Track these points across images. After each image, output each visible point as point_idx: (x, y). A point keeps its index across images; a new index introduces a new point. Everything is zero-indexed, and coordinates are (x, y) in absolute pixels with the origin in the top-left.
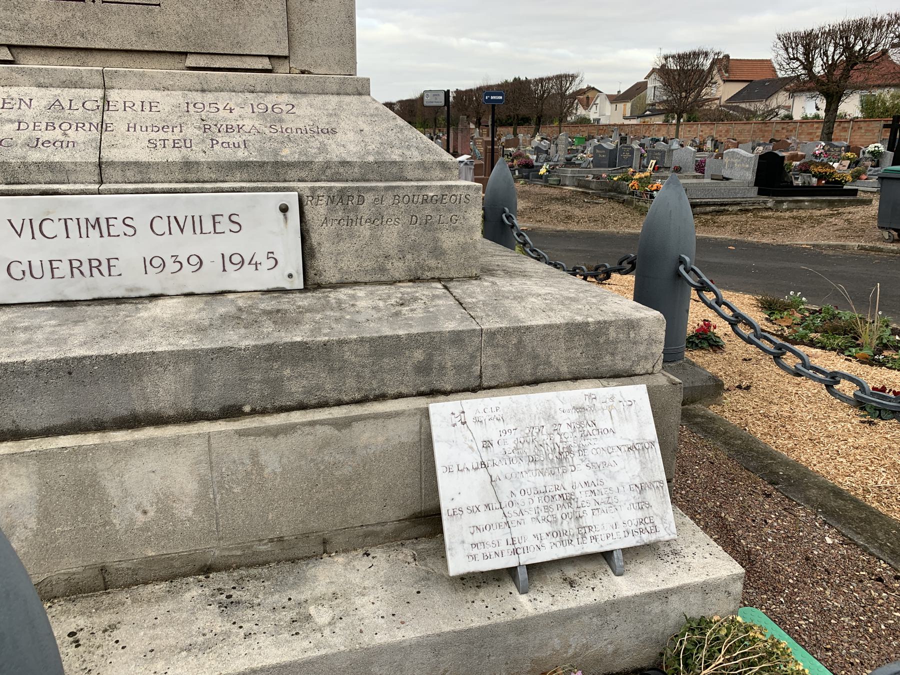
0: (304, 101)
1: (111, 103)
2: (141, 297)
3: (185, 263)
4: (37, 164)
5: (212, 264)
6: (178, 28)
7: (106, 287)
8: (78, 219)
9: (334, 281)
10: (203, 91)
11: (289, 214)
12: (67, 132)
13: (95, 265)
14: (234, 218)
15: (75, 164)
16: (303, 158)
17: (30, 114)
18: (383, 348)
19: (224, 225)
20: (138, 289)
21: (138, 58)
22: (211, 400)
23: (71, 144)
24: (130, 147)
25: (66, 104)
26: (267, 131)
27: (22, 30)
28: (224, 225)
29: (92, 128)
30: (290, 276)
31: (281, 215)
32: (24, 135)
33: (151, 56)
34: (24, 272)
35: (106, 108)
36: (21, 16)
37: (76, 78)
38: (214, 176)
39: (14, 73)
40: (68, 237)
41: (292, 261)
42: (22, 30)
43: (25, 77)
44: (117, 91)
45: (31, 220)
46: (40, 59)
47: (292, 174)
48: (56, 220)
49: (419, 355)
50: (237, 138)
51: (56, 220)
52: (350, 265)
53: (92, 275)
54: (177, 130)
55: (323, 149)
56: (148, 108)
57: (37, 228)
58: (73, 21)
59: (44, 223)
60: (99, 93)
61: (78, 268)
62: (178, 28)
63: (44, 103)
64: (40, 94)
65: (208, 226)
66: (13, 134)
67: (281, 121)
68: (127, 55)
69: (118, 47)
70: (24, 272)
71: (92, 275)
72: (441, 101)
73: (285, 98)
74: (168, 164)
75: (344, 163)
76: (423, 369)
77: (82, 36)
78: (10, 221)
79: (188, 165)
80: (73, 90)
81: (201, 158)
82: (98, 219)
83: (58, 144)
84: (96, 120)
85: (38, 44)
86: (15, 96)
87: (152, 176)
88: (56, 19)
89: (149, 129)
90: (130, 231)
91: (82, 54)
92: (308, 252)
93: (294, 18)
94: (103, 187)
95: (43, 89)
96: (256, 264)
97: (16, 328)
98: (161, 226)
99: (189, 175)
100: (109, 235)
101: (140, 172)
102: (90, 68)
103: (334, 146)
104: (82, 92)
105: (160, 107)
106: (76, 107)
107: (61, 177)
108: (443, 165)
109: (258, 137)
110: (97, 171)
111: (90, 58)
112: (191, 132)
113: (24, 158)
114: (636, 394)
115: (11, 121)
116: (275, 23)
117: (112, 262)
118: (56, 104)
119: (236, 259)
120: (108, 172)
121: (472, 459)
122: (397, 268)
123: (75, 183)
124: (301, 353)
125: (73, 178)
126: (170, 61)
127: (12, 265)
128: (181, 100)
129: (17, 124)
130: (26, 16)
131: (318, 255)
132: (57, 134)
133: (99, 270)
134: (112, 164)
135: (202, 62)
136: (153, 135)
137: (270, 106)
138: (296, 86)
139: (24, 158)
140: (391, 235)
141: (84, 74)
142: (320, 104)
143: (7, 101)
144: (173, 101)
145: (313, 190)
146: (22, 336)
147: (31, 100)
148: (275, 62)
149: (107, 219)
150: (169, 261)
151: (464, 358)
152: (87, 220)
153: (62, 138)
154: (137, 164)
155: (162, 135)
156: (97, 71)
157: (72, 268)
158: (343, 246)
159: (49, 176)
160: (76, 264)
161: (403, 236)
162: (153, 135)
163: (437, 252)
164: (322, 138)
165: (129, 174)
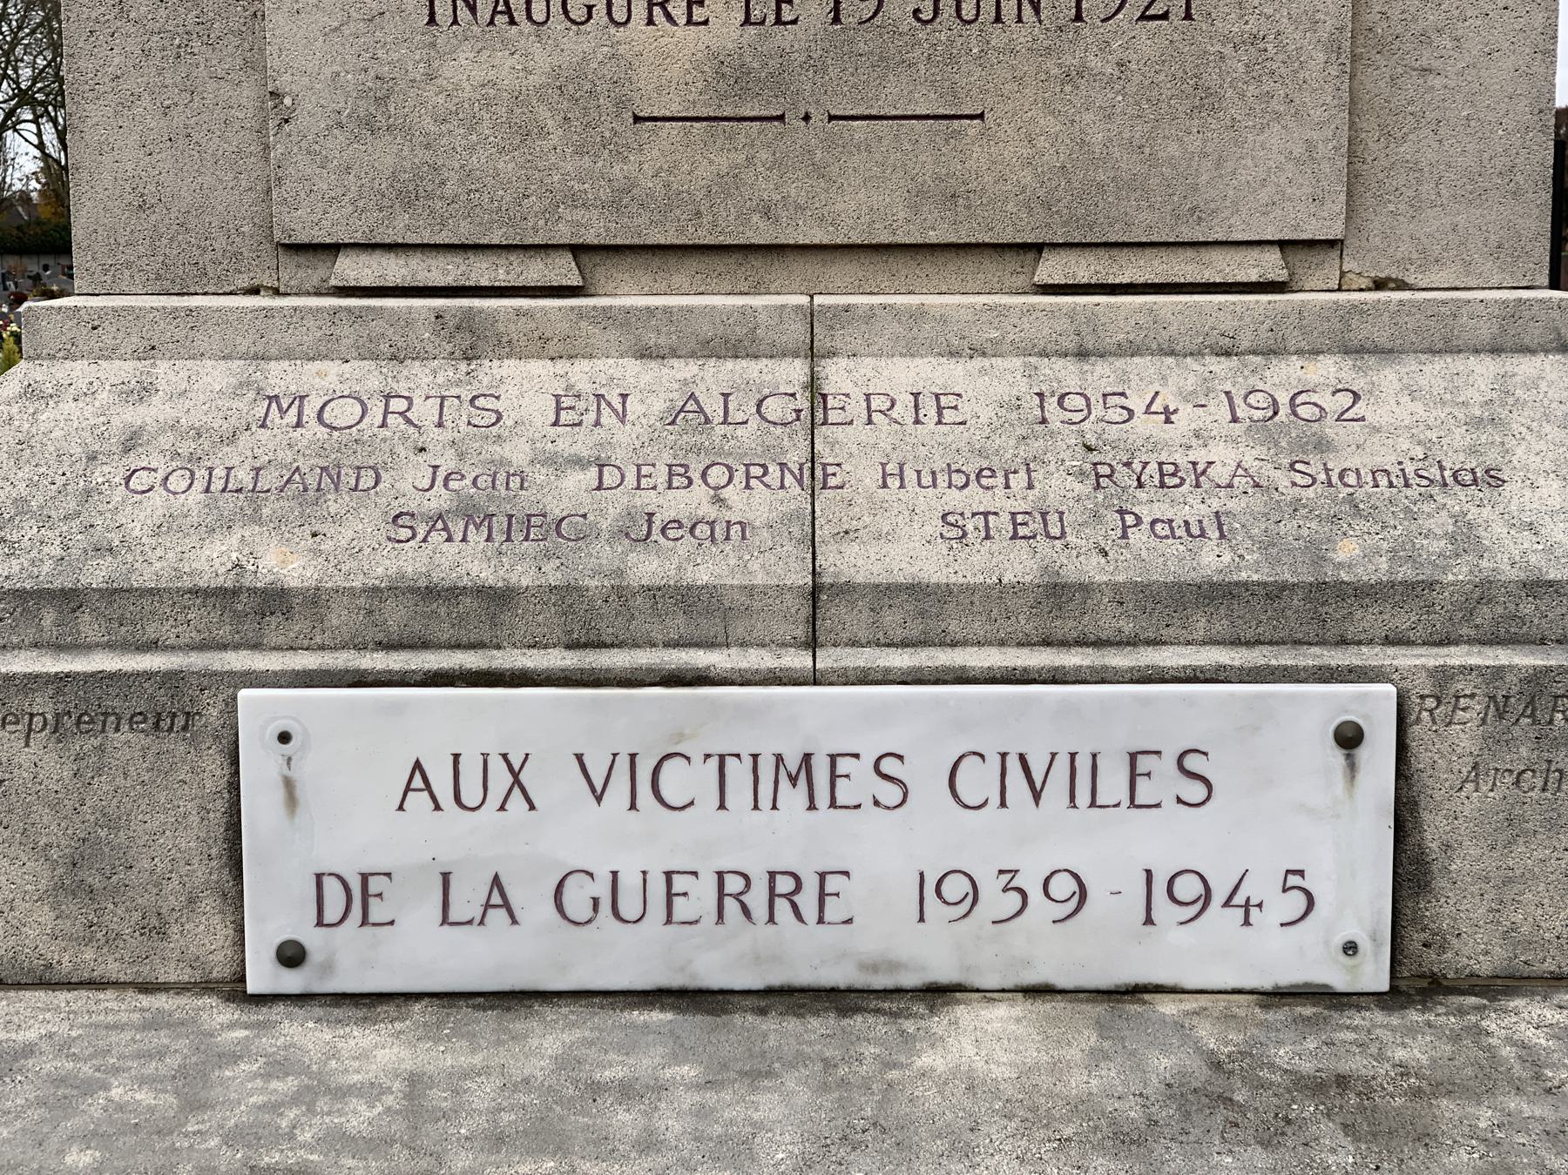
0: (1388, 377)
1: (831, 402)
2: (899, 991)
3: (1035, 894)
4: (652, 592)
5: (1114, 902)
6: (1027, 177)
7: (809, 955)
8: (755, 757)
9: (1485, 967)
10: (1082, 354)
11: (1363, 753)
12: (725, 493)
13: (784, 889)
14: (1192, 763)
15: (749, 590)
16: (1405, 572)
17: (625, 440)
19: (1162, 782)
20: (894, 966)
21: (903, 267)
23: (735, 530)
24: (898, 543)
25: (714, 407)
26: (1282, 479)
27: (615, 205)
28: (1162, 782)
29: (789, 480)
30: (1350, 948)
31: (1337, 757)
32: (614, 505)
33: (940, 258)
34: (596, 902)
35: (819, 415)
36: (617, 168)
37: (740, 331)
38: (1128, 627)
39: (583, 324)
40: (722, 806)
41: (1359, 898)
42: (615, 205)
43: (613, 334)
44: (843, 362)
45: (633, 756)
46: (646, 280)
47: (1368, 619)
48: (697, 758)
50: (1192, 507)
51: (697, 758)
53: (771, 920)
54: (1019, 481)
55: (1465, 538)
56: (933, 412)
57: (645, 778)
58: (748, 176)
59: (667, 765)
60: (797, 370)
61: (737, 896)
62: (1027, 177)
63: (659, 406)
64: (646, 378)
65: (1113, 784)
66: (587, 502)
67: (1323, 445)
68: (876, 258)
69: (856, 239)
70: (596, 901)
71: (771, 920)
73: (1327, 369)
74: (1000, 592)
75: (1536, 587)
77: (766, 214)
78: (579, 757)
79: (1058, 593)
80: (730, 364)
81: (1092, 569)
82: (807, 758)
83: (703, 530)
84: (796, 456)
85: (649, 241)
86: (584, 386)
87: (953, 626)
88: (705, 171)
89: (942, 480)
90: (891, 794)
91: (757, 261)
92: (1411, 874)
93: (1369, 124)
94: (827, 659)
95: (653, 364)
96: (1247, 906)
97: (596, 1089)
98: (978, 781)
100: (833, 804)
101: (922, 614)
102: (777, 301)
103: (1499, 529)
104: (752, 369)
105: (966, 410)
106: (740, 417)
107: (712, 627)
109: (1257, 501)
110: (806, 611)
111: (777, 271)
112: (1060, 486)
113: (620, 573)
115: (579, 463)
116: (1310, 146)
117: (832, 884)
118: (686, 411)
119: (1188, 888)
120: (834, 613)
123: (743, 644)
125: (739, 630)
126: (991, 269)
127: (568, 882)
128: (1022, 386)
129: (594, 470)
130: (630, 168)
131: (1440, 883)
132: (692, 501)
133: (794, 906)
134: (846, 590)
135: (1083, 268)
136: (954, 499)
137: (1283, 398)
138: (1363, 331)
139: (620, 573)
141: (762, 318)
142: (1439, 386)
143: (566, 402)
144: (1003, 391)
145: (1443, 676)
146: (625, 1120)
147: (624, 396)
148: (1298, 257)
149: (833, 758)
150: (990, 887)
152: (779, 758)
153: (711, 512)
154: (915, 590)
155: (975, 498)
156: (798, 308)
157: (721, 895)
158: (1523, 856)
159: (678, 624)
160: (734, 884)
162: (954, 499)
164: (1457, 500)
165: (891, 619)
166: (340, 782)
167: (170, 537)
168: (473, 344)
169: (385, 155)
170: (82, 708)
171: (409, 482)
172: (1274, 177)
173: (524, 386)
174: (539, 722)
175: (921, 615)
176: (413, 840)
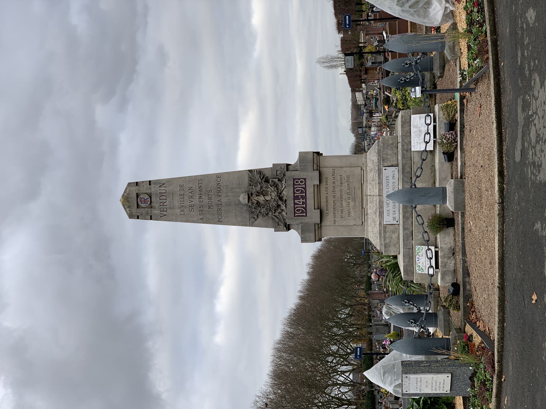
5: (394, 181)
18: (403, 157)
19: (388, 178)
22: (409, 181)
24: (377, 191)
28: (388, 178)
49: (405, 152)
52: (394, 159)
55: (376, 162)
57: (388, 204)
76: (407, 151)
79: (379, 183)
92: (392, 166)
99: (380, 183)
102: (365, 198)
108: (378, 142)
112: (374, 183)
114: (413, 116)
121: (419, 145)
122: (395, 151)
140: (390, 152)
151: (406, 145)
161: (390, 150)
163: (393, 144)
166: (388, 219)
167: (377, 229)
168: (367, 214)
169: (357, 219)
170: (385, 232)
171: (374, 217)
172: (358, 171)
173: (369, 211)
174: (385, 209)
175: (380, 190)
176: (391, 216)
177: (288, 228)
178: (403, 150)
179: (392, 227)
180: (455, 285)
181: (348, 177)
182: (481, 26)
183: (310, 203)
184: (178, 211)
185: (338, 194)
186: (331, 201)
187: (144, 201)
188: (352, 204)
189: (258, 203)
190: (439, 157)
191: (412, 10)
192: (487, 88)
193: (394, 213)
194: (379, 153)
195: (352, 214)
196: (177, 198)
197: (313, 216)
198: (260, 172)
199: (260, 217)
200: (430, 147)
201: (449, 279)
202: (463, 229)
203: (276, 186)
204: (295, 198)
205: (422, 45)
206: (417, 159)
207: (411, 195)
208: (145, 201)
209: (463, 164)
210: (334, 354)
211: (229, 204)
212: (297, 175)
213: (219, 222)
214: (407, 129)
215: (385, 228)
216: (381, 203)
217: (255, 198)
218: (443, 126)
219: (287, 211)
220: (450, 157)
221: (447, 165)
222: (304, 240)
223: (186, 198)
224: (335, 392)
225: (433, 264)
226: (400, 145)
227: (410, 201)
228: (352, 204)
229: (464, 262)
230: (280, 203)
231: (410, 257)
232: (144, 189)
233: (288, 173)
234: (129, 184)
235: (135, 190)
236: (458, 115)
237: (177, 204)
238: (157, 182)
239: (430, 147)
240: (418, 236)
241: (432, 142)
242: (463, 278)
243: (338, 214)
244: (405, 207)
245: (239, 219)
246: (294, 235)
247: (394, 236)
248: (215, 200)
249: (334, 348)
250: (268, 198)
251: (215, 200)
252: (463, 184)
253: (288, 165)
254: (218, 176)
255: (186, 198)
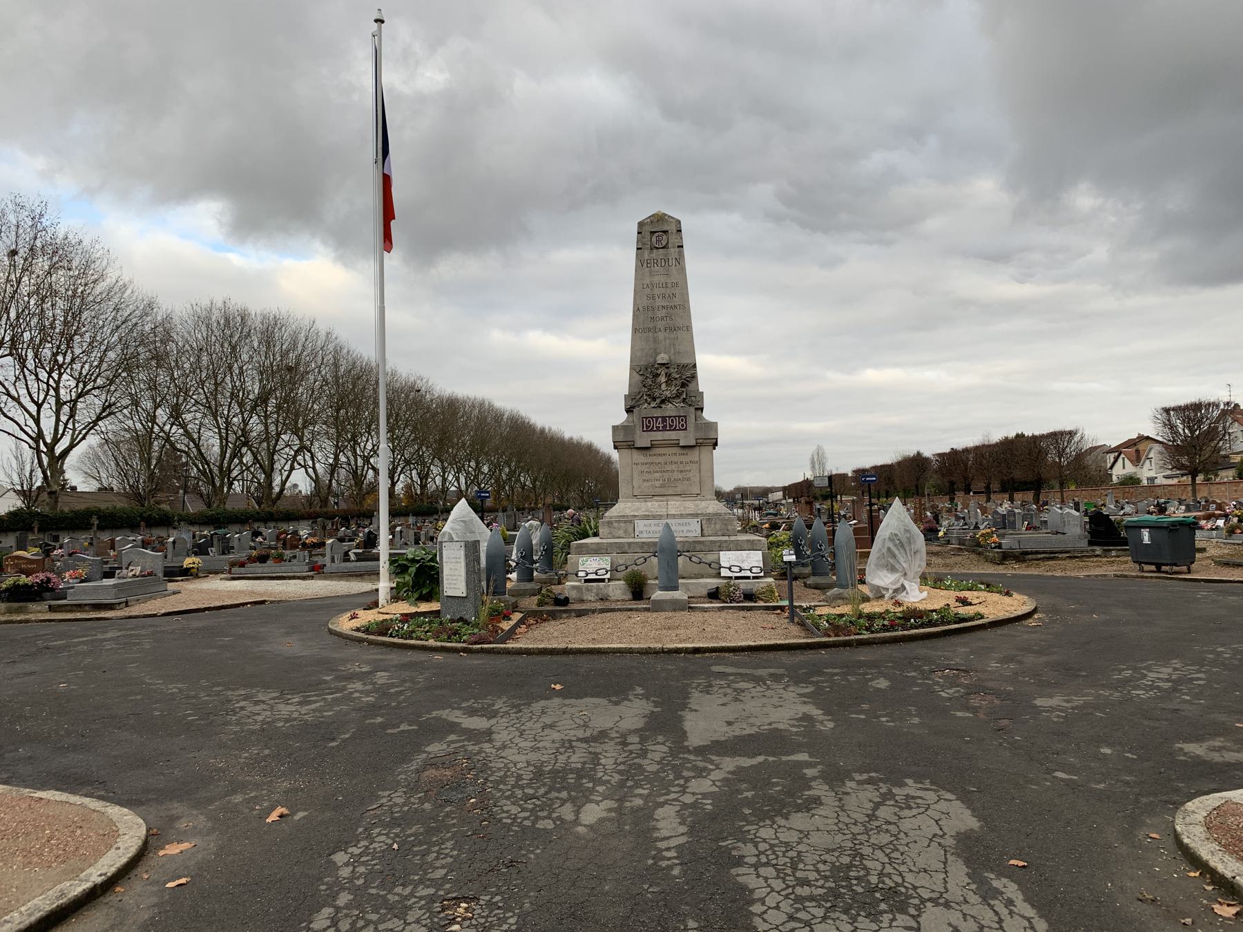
18: (712, 542)
24: (672, 512)
72: (826, 483)
99: (682, 516)
114: (760, 553)
124: (699, 542)
140: (718, 526)
166: (640, 525)
167: (628, 512)
172: (696, 490)
175: (674, 516)
176: (644, 529)
177: (629, 410)
178: (721, 542)
179: (631, 529)
180: (566, 601)
181: (688, 479)
182: (867, 629)
183: (659, 436)
184: (647, 281)
185: (669, 467)
186: (660, 459)
187: (659, 240)
188: (658, 484)
189: (658, 375)
190: (713, 582)
191: (885, 551)
192: (795, 636)
193: (648, 532)
194: (716, 514)
195: (646, 484)
196: (662, 279)
197: (643, 440)
198: (694, 377)
199: (641, 378)
200: (724, 573)
201: (573, 595)
202: (631, 610)
203: (678, 396)
204: (664, 419)
205: (844, 561)
206: (710, 557)
207: (669, 551)
208: (658, 241)
209: (705, 610)
210: (478, 468)
211: (655, 341)
212: (691, 420)
213: (635, 330)
214: (745, 546)
215: (630, 522)
216: (660, 517)
217: (663, 371)
218: (749, 587)
219: (648, 409)
220: (714, 595)
221: (704, 592)
222: (615, 428)
223: (663, 291)
224: (435, 470)
225: (590, 577)
226: (726, 538)
227: (662, 550)
228: (658, 484)
229: (594, 611)
230: (658, 401)
231: (597, 551)
232: (673, 240)
233: (692, 409)
234: (679, 222)
235: (672, 228)
236: (762, 604)
237: (656, 279)
238: (681, 255)
239: (724, 573)
240: (621, 559)
241: (730, 574)
242: (575, 611)
243: (645, 468)
244: (654, 544)
245: (639, 354)
246: (621, 417)
247: (621, 533)
248: (660, 324)
249: (485, 469)
250: (663, 387)
251: (660, 324)
252: (683, 610)
253: (702, 409)
254: (689, 328)
255: (663, 291)
